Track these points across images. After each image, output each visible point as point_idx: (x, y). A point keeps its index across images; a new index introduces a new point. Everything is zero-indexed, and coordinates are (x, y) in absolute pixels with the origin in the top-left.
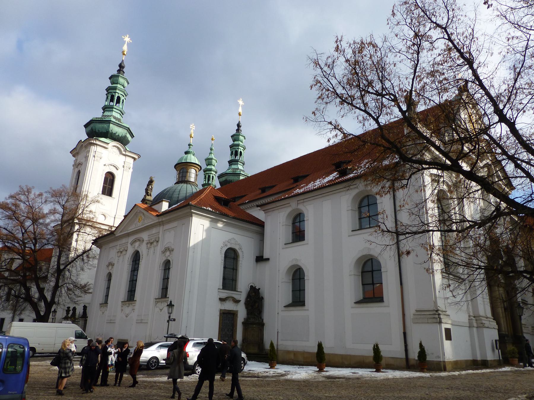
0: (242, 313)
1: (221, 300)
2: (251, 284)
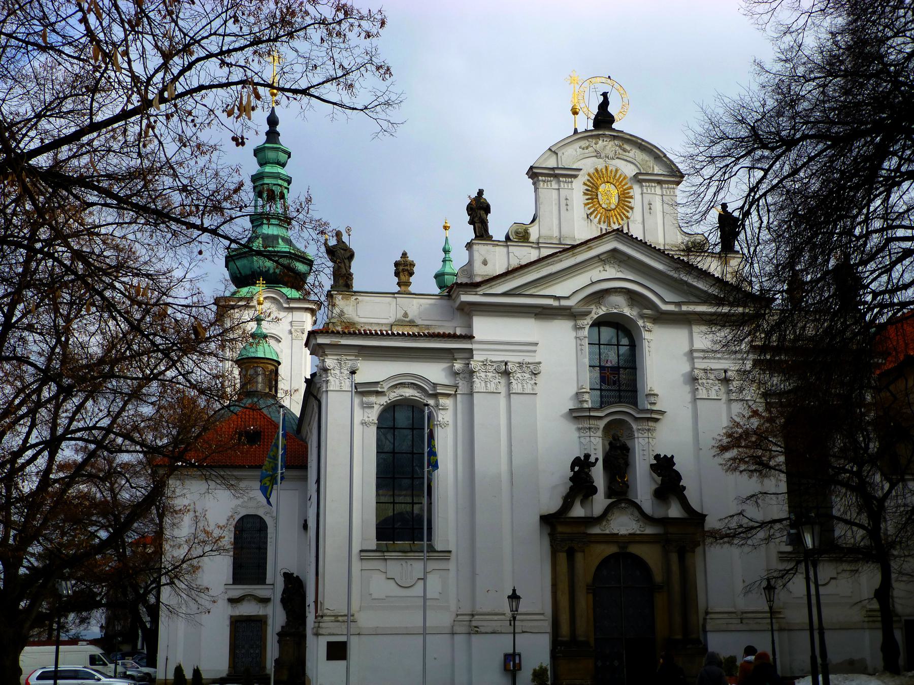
0: (276, 617)
1: (232, 601)
2: (287, 571)
